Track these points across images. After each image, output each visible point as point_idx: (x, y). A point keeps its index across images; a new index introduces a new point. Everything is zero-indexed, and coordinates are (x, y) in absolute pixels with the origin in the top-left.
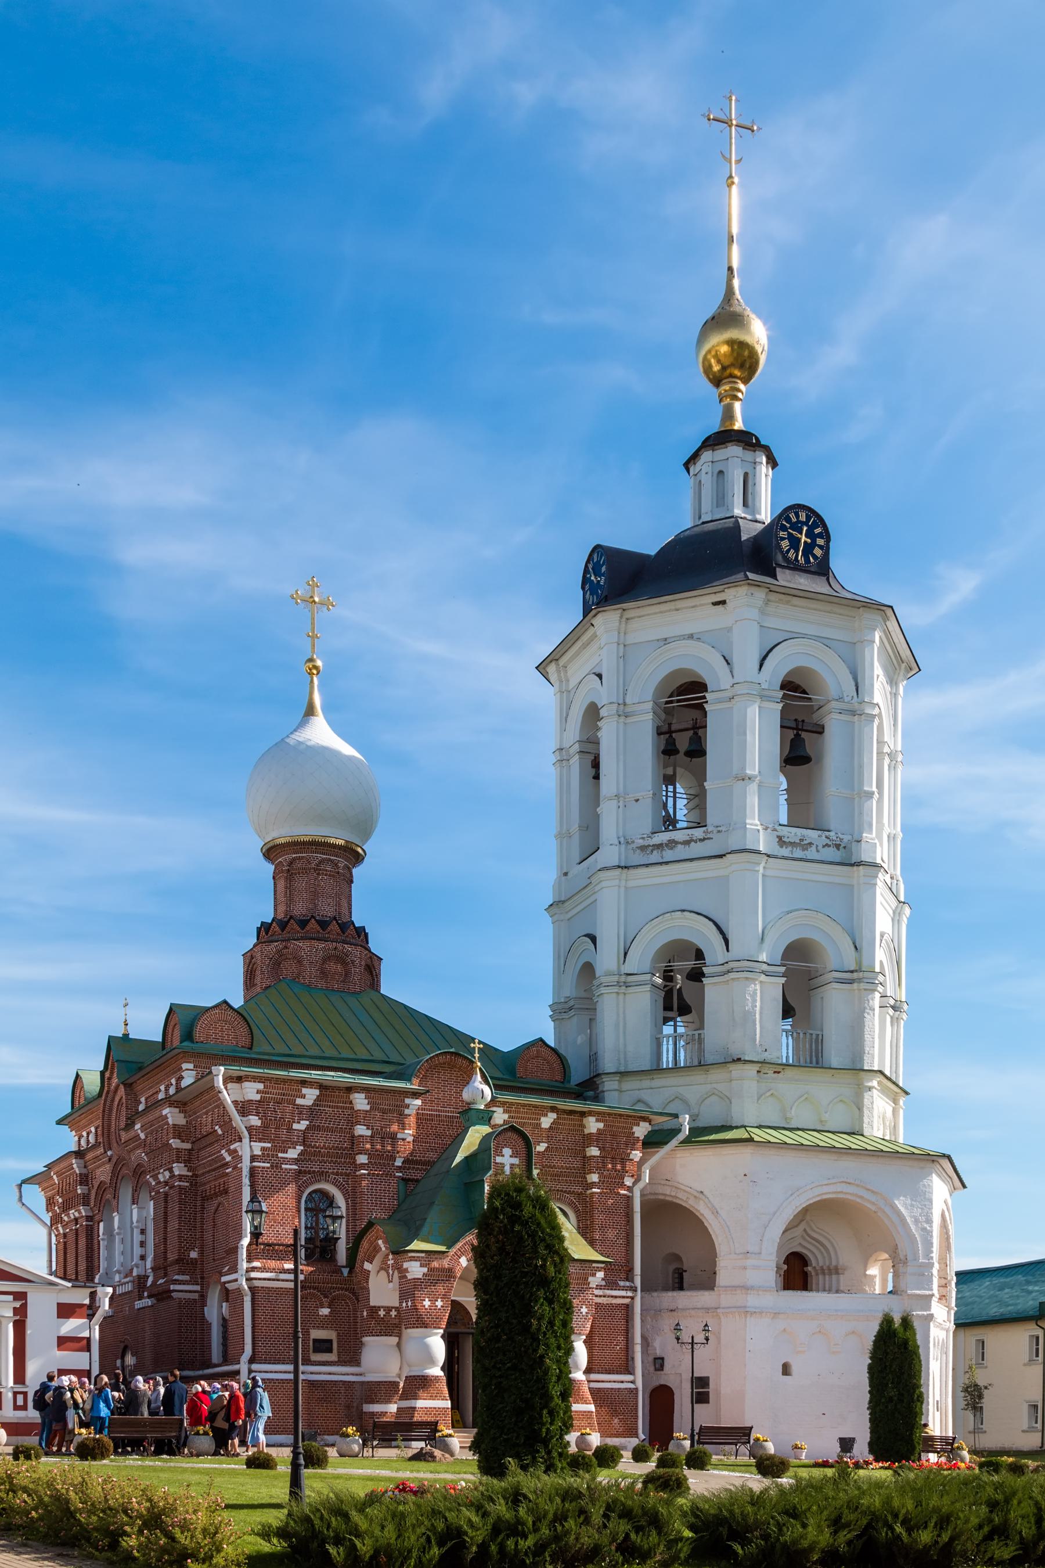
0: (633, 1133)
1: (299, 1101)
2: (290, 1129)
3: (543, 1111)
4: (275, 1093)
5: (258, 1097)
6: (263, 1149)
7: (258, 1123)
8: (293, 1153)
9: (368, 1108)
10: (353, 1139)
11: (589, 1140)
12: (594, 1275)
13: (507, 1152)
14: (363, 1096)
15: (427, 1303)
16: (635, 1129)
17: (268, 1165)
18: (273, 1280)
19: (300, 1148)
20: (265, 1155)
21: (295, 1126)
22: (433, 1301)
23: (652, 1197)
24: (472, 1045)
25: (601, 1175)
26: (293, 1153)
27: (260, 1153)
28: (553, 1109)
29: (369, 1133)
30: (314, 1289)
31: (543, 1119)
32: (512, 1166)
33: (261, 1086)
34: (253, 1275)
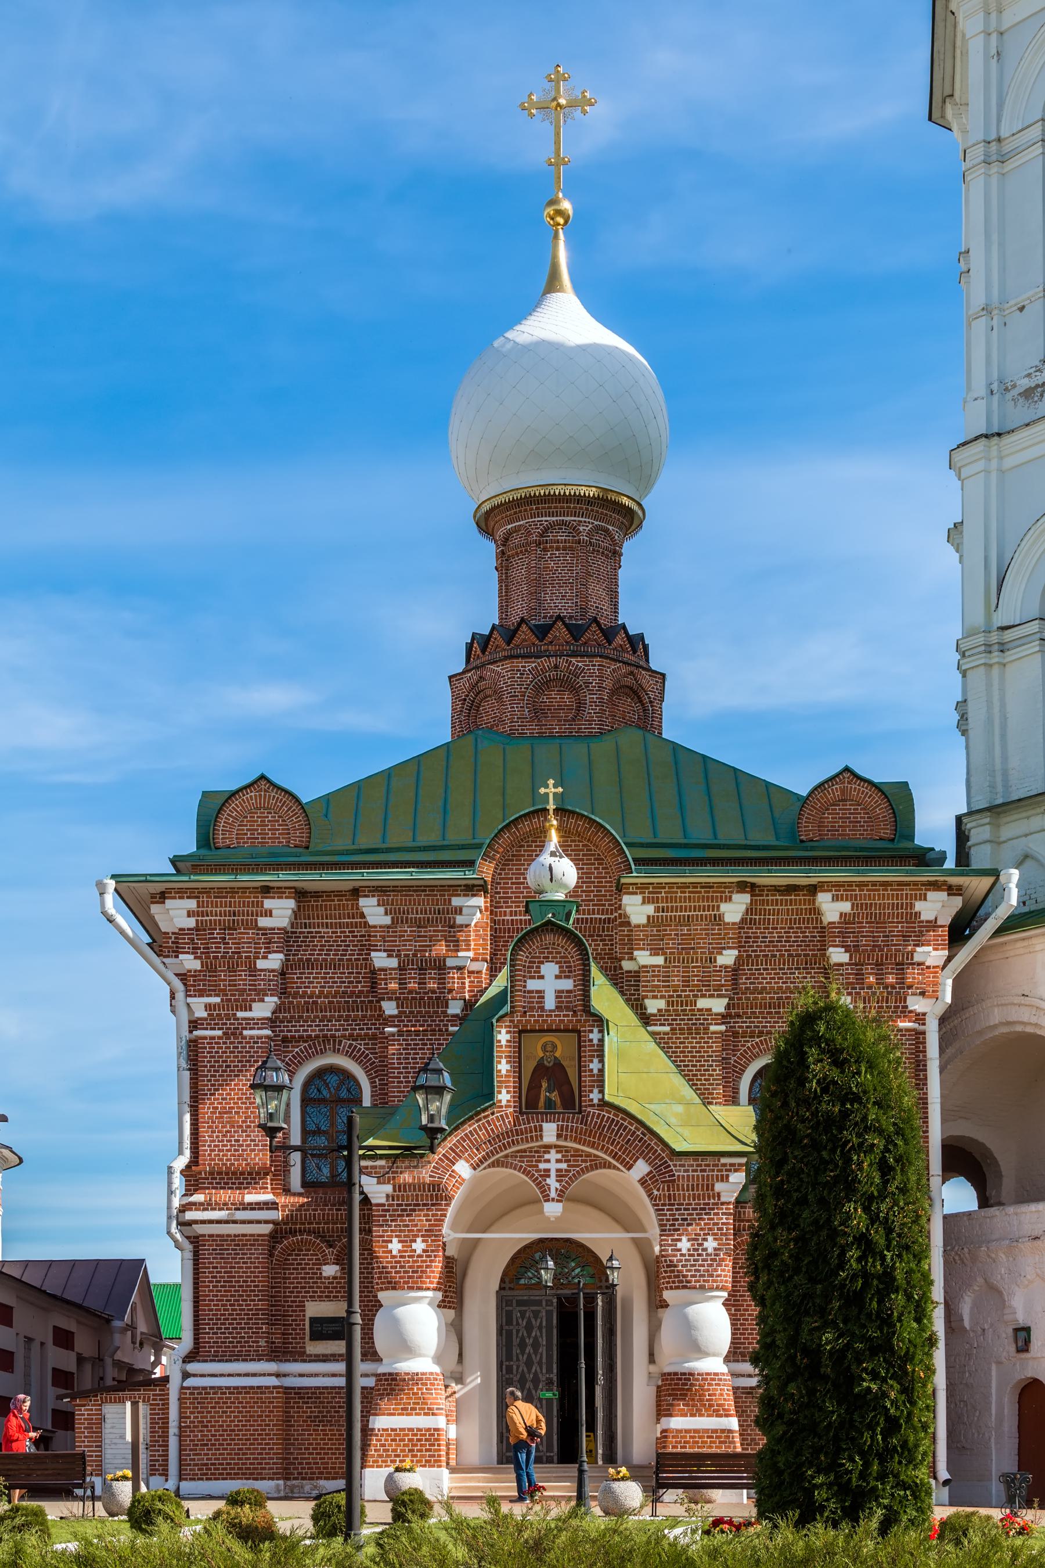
1: (263, 922)
2: (253, 970)
3: (724, 893)
4: (218, 912)
5: (191, 923)
6: (208, 1007)
7: (196, 965)
8: (263, 1009)
9: (387, 920)
10: (374, 975)
11: (824, 935)
12: (725, 1179)
14: (374, 901)
15: (395, 1246)
16: (919, 906)
17: (220, 1033)
18: (227, 1222)
19: (272, 1001)
20: (214, 1016)
21: (261, 964)
22: (407, 1241)
23: (1005, 1030)
24: (542, 791)
27: (205, 1014)
28: (742, 887)
29: (393, 963)
30: (309, 1233)
31: (724, 907)
33: (192, 904)
34: (190, 1215)
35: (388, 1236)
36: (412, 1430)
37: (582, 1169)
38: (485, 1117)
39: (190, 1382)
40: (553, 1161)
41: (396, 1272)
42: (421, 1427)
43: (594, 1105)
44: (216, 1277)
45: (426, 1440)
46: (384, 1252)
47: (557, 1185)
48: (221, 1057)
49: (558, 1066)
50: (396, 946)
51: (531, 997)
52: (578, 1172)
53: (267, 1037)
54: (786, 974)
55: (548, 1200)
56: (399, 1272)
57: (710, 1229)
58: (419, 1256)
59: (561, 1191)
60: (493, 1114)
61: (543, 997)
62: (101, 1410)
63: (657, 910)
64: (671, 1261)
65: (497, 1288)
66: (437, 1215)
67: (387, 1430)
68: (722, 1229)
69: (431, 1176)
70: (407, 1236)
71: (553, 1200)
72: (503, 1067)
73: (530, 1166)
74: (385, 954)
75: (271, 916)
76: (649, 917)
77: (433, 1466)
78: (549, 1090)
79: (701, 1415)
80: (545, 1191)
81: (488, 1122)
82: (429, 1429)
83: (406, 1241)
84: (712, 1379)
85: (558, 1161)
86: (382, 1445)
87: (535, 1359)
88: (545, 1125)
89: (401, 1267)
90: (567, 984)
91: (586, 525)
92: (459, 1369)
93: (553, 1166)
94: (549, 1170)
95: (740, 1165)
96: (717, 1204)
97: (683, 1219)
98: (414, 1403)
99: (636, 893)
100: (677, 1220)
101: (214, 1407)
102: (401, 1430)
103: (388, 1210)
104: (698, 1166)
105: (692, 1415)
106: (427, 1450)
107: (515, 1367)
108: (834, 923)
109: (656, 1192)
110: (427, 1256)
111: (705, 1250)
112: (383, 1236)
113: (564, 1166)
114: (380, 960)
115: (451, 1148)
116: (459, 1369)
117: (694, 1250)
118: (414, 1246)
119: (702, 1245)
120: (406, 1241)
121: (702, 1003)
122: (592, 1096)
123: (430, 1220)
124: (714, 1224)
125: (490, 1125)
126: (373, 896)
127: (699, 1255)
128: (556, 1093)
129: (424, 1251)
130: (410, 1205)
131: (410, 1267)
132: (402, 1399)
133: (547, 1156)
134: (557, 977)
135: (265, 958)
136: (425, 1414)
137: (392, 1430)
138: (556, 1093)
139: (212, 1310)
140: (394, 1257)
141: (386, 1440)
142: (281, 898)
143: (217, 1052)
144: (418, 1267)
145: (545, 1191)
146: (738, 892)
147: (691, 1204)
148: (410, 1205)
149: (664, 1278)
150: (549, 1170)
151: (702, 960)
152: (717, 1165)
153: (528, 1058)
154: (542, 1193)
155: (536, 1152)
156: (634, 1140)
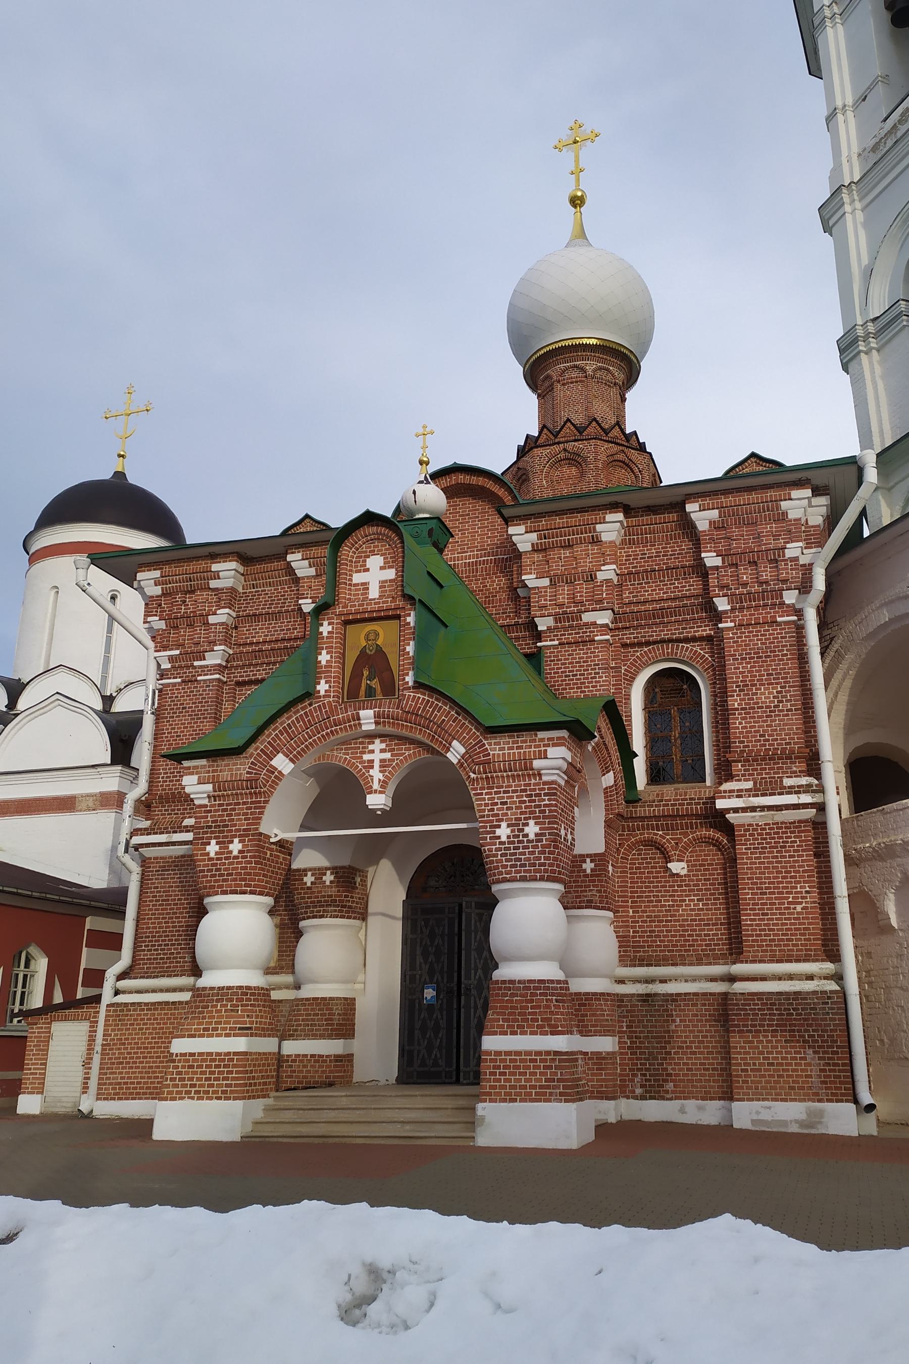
0: (785, 514)
1: (213, 584)
6: (171, 659)
8: (214, 658)
13: (375, 562)
14: (298, 556)
15: (213, 848)
17: (179, 680)
21: (212, 619)
22: (224, 844)
25: (732, 598)
26: (214, 658)
27: (169, 666)
32: (382, 584)
33: (157, 574)
36: (211, 1054)
38: (303, 709)
39: (121, 999)
40: (377, 751)
43: (409, 688)
44: (156, 896)
46: (202, 855)
48: (180, 701)
49: (379, 651)
51: (356, 590)
53: (219, 680)
54: (666, 585)
55: (370, 793)
58: (236, 857)
60: (310, 705)
61: (368, 589)
62: (50, 1028)
63: (540, 538)
67: (185, 1055)
69: (248, 773)
70: (226, 837)
71: (376, 791)
75: (219, 578)
76: (533, 544)
78: (370, 678)
79: (523, 1033)
82: (229, 1054)
83: (224, 842)
85: (382, 751)
88: (362, 713)
91: (590, 366)
93: (377, 757)
96: (538, 784)
97: (502, 803)
98: (216, 1023)
99: (520, 525)
100: (496, 804)
101: (133, 1024)
102: (200, 1054)
103: (210, 811)
104: (513, 743)
105: (514, 1033)
106: (224, 1079)
109: (472, 775)
110: (243, 857)
113: (388, 755)
115: (269, 743)
117: (514, 836)
118: (231, 847)
119: (522, 830)
120: (224, 842)
121: (587, 617)
125: (307, 716)
126: (299, 552)
127: (519, 842)
129: (240, 852)
130: (231, 804)
131: (225, 870)
132: (204, 1018)
133: (371, 747)
134: (382, 568)
139: (149, 928)
140: (211, 859)
141: (184, 1067)
143: (177, 697)
144: (233, 869)
147: (511, 786)
148: (231, 804)
151: (583, 578)
152: (535, 741)
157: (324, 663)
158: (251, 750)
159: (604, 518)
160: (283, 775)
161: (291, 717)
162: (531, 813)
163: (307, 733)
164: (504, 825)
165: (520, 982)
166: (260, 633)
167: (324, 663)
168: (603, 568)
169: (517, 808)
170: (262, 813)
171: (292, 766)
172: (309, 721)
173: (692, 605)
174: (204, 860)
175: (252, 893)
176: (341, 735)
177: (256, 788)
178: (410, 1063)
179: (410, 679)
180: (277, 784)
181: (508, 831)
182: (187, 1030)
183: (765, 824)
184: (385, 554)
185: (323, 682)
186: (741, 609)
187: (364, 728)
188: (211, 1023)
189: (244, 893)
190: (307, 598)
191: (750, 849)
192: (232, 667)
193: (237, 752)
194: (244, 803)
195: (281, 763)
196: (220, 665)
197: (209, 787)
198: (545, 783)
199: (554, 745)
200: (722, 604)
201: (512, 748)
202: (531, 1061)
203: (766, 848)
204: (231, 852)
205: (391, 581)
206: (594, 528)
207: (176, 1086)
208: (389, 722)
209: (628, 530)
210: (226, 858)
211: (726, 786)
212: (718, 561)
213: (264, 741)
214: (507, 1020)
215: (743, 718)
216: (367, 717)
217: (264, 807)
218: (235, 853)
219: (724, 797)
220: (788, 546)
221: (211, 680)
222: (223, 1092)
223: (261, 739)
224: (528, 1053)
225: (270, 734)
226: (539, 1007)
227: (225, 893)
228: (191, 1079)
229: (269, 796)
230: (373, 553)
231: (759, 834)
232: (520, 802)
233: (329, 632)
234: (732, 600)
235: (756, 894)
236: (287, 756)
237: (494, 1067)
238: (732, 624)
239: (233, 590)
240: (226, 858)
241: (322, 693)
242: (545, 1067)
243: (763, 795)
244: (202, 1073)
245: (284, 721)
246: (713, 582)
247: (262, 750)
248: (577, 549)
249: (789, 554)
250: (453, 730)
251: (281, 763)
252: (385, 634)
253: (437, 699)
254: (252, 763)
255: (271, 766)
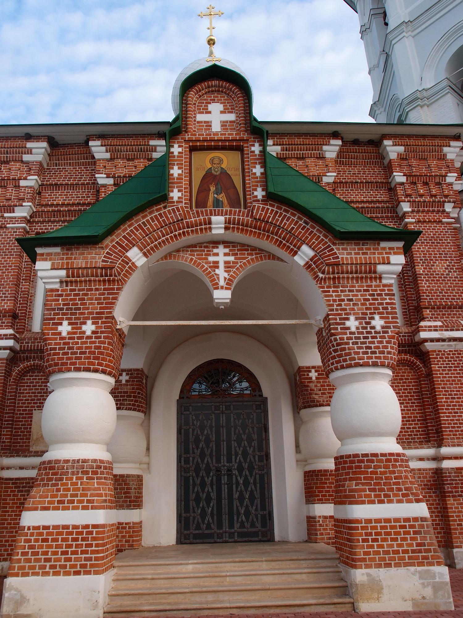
0: (445, 155)
1: (26, 158)
2: (18, 187)
8: (22, 212)
9: (108, 156)
13: (216, 108)
14: (98, 143)
15: (65, 328)
21: (23, 183)
22: (76, 324)
25: (412, 203)
26: (22, 212)
29: (111, 181)
35: (58, 319)
36: (66, 527)
37: (248, 261)
38: (157, 210)
40: (221, 254)
41: (64, 354)
42: (77, 523)
43: (258, 201)
45: (83, 539)
46: (53, 334)
47: (226, 275)
49: (224, 173)
50: (113, 171)
52: (244, 264)
53: (24, 228)
54: (365, 193)
55: (217, 288)
56: (67, 353)
57: (375, 309)
58: (88, 337)
59: (229, 280)
60: (165, 207)
61: (211, 126)
63: (283, 150)
64: (341, 339)
65: (177, 397)
66: (108, 298)
67: (38, 528)
68: (387, 308)
69: (103, 261)
71: (222, 288)
72: (175, 172)
73: (200, 259)
74: (105, 176)
75: (31, 154)
76: (277, 154)
77: (89, 573)
79: (390, 501)
80: (214, 280)
81: (160, 215)
82: (87, 526)
84: (396, 460)
85: (226, 254)
86: (31, 547)
87: (207, 452)
88: (214, 218)
89: (69, 348)
90: (231, 117)
92: (146, 460)
94: (217, 262)
95: (398, 248)
96: (379, 286)
97: (348, 300)
98: (72, 496)
100: (343, 300)
102: (55, 527)
103: (61, 295)
104: (359, 249)
105: (381, 502)
106: (83, 552)
107: (191, 459)
108: (394, 160)
109: (321, 275)
110: (96, 338)
111: (373, 328)
112: (54, 319)
113: (231, 258)
114: (102, 179)
115: (124, 237)
116: (146, 460)
117: (364, 328)
118: (84, 328)
119: (369, 323)
122: (256, 193)
123: (102, 303)
124: (379, 304)
128: (223, 194)
129: (93, 332)
130: (83, 290)
131: (78, 348)
132: (58, 490)
133: (215, 251)
135: (25, 179)
136: (85, 508)
137: (45, 528)
138: (223, 194)
140: (64, 338)
141: (36, 540)
142: (39, 141)
145: (214, 280)
146: (333, 139)
147: (354, 286)
148: (83, 290)
149: (334, 357)
150: (217, 262)
152: (377, 249)
153: (197, 169)
154: (211, 281)
155: (205, 247)
156: (298, 229)
157: (176, 175)
158: (107, 241)
159: (329, 142)
160: (136, 267)
161: (146, 216)
162: (375, 309)
163: (161, 231)
164: (352, 318)
165: (383, 455)
166: (59, 198)
167: (176, 175)
168: (328, 174)
169: (362, 304)
170: (116, 299)
171: (144, 260)
172: (164, 221)
173: (383, 207)
174: (56, 339)
175: (103, 372)
176: (191, 236)
177: (111, 275)
178: (187, 527)
179: (259, 193)
180: (130, 274)
181: (357, 323)
182: (40, 502)
183: (450, 351)
184: (225, 103)
185: (176, 190)
186: (418, 212)
187: (214, 232)
188: (66, 496)
189: (96, 371)
190: (102, 173)
191: (441, 367)
192: (34, 222)
193: (92, 241)
194: (97, 290)
195: (135, 255)
196: (25, 218)
197: (63, 273)
198: (384, 286)
199: (395, 253)
200: (406, 207)
201: (358, 254)
202: (401, 527)
203: (452, 367)
204: (84, 332)
205: (231, 122)
206: (322, 148)
207: (29, 561)
208: (238, 228)
209: (340, 154)
210: (79, 338)
211: (422, 324)
212: (403, 179)
213: (119, 235)
214: (374, 490)
215: (427, 281)
216: (218, 221)
217: (117, 294)
218: (89, 333)
219: (425, 330)
220: (449, 175)
221: (17, 228)
222: (82, 566)
223: (117, 232)
224: (397, 520)
225: (126, 229)
226: (401, 477)
227: (78, 370)
228: (46, 553)
229: (122, 284)
230: (213, 101)
231: (446, 358)
232: (364, 300)
233: (179, 153)
234: (413, 205)
235: (448, 398)
236: (141, 250)
237: (366, 534)
238: (414, 220)
239: (41, 164)
240: (79, 338)
241: (176, 199)
242: (415, 532)
243: (452, 330)
244: (57, 546)
245: (140, 220)
246: (400, 191)
247: (117, 243)
248: (309, 161)
249: (449, 180)
250: (303, 236)
251: (135, 255)
252: (229, 161)
253: (286, 211)
254: (107, 253)
255: (126, 257)
